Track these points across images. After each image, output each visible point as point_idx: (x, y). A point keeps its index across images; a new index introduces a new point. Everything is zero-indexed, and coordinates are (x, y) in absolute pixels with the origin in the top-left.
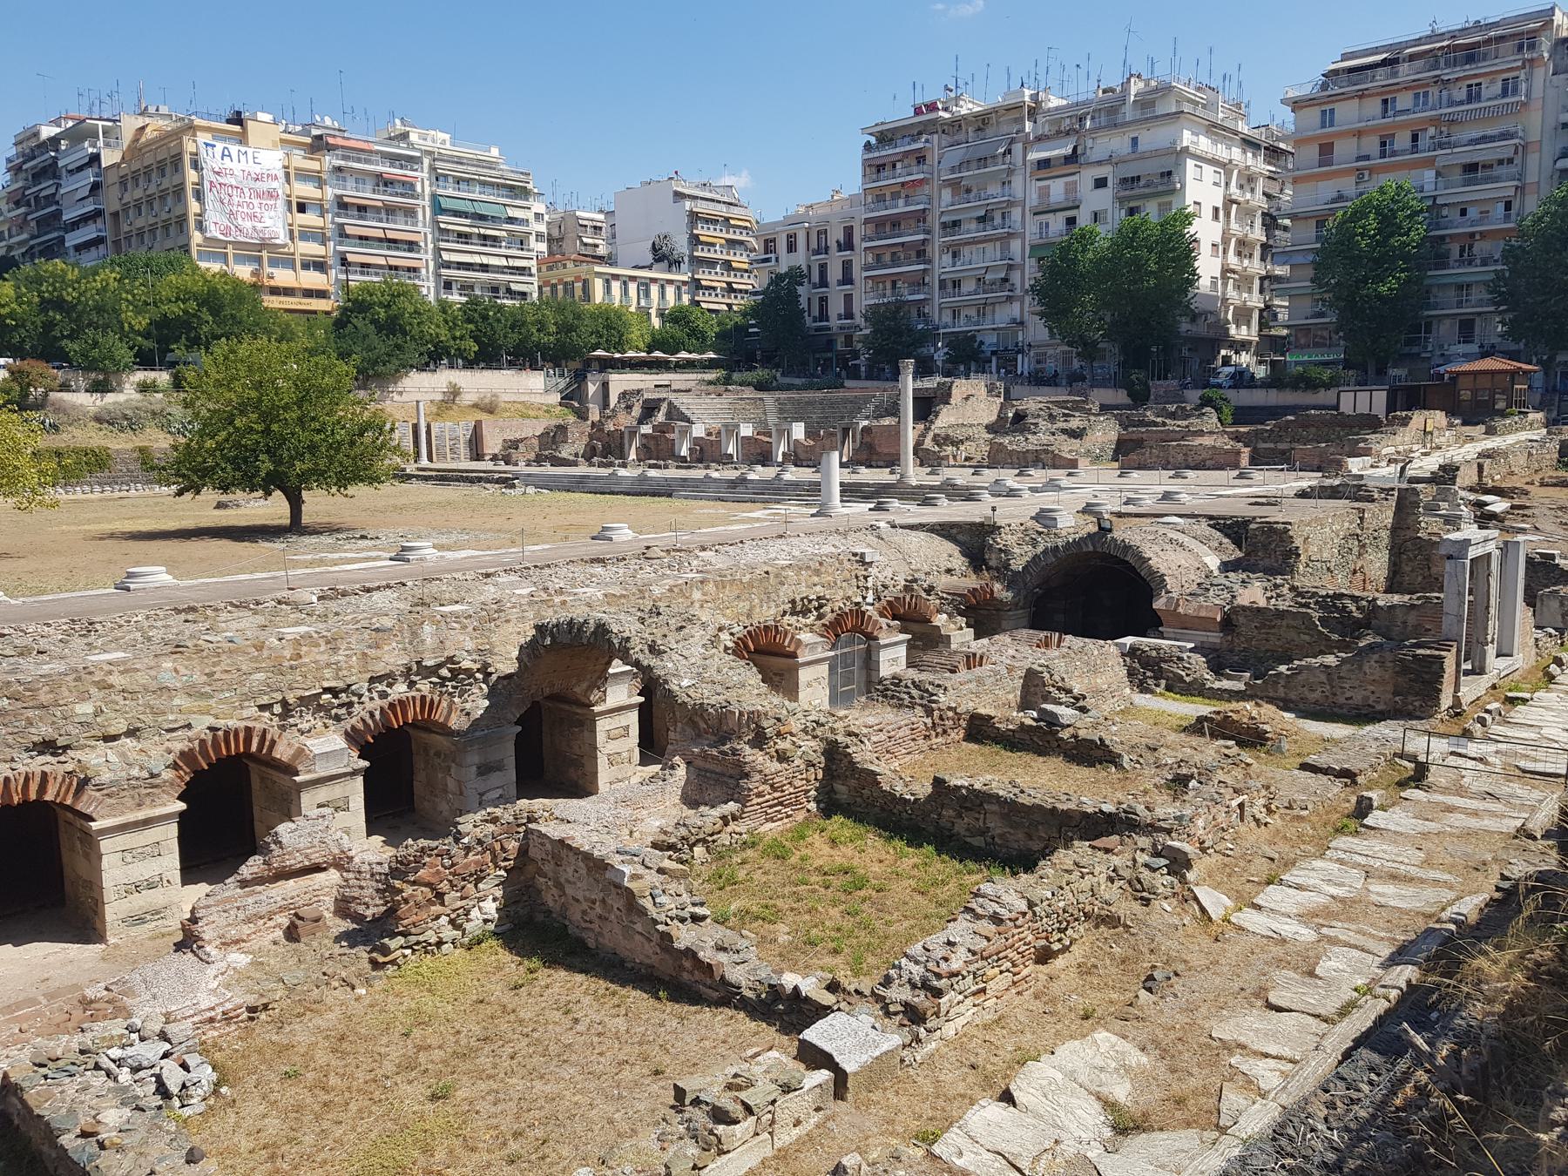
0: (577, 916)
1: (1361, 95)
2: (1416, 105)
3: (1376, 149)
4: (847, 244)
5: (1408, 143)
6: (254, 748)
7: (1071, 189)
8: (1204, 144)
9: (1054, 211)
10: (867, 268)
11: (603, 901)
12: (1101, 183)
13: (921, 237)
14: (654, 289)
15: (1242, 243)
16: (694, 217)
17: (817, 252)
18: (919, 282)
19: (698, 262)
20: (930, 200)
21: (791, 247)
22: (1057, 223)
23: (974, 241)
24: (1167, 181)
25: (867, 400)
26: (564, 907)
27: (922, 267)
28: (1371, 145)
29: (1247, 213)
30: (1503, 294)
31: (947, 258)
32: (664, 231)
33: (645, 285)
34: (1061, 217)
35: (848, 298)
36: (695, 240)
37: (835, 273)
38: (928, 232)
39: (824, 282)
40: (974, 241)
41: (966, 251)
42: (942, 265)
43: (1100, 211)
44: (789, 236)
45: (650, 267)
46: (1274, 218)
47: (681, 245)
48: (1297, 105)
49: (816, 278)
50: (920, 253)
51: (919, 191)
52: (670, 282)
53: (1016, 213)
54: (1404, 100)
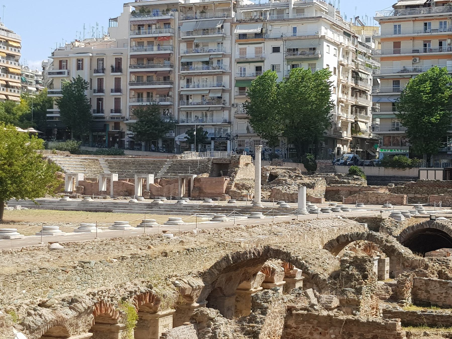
1: (415, 20)
2: (441, 27)
3: (421, 47)
4: (117, 68)
5: (437, 46)
7: (259, 51)
8: (329, 34)
9: (249, 62)
10: (131, 84)
12: (276, 50)
13: (168, 69)
15: (344, 87)
17: (97, 71)
20: (173, 48)
21: (79, 67)
22: (250, 69)
23: (202, 75)
24: (313, 54)
27: (169, 86)
28: (419, 45)
29: (346, 70)
31: (183, 83)
37: (109, 84)
38: (171, 66)
39: (100, 90)
40: (202, 75)
42: (180, 85)
43: (277, 67)
46: (357, 74)
48: (382, 21)
50: (166, 78)
51: (165, 43)
53: (226, 61)
54: (435, 25)
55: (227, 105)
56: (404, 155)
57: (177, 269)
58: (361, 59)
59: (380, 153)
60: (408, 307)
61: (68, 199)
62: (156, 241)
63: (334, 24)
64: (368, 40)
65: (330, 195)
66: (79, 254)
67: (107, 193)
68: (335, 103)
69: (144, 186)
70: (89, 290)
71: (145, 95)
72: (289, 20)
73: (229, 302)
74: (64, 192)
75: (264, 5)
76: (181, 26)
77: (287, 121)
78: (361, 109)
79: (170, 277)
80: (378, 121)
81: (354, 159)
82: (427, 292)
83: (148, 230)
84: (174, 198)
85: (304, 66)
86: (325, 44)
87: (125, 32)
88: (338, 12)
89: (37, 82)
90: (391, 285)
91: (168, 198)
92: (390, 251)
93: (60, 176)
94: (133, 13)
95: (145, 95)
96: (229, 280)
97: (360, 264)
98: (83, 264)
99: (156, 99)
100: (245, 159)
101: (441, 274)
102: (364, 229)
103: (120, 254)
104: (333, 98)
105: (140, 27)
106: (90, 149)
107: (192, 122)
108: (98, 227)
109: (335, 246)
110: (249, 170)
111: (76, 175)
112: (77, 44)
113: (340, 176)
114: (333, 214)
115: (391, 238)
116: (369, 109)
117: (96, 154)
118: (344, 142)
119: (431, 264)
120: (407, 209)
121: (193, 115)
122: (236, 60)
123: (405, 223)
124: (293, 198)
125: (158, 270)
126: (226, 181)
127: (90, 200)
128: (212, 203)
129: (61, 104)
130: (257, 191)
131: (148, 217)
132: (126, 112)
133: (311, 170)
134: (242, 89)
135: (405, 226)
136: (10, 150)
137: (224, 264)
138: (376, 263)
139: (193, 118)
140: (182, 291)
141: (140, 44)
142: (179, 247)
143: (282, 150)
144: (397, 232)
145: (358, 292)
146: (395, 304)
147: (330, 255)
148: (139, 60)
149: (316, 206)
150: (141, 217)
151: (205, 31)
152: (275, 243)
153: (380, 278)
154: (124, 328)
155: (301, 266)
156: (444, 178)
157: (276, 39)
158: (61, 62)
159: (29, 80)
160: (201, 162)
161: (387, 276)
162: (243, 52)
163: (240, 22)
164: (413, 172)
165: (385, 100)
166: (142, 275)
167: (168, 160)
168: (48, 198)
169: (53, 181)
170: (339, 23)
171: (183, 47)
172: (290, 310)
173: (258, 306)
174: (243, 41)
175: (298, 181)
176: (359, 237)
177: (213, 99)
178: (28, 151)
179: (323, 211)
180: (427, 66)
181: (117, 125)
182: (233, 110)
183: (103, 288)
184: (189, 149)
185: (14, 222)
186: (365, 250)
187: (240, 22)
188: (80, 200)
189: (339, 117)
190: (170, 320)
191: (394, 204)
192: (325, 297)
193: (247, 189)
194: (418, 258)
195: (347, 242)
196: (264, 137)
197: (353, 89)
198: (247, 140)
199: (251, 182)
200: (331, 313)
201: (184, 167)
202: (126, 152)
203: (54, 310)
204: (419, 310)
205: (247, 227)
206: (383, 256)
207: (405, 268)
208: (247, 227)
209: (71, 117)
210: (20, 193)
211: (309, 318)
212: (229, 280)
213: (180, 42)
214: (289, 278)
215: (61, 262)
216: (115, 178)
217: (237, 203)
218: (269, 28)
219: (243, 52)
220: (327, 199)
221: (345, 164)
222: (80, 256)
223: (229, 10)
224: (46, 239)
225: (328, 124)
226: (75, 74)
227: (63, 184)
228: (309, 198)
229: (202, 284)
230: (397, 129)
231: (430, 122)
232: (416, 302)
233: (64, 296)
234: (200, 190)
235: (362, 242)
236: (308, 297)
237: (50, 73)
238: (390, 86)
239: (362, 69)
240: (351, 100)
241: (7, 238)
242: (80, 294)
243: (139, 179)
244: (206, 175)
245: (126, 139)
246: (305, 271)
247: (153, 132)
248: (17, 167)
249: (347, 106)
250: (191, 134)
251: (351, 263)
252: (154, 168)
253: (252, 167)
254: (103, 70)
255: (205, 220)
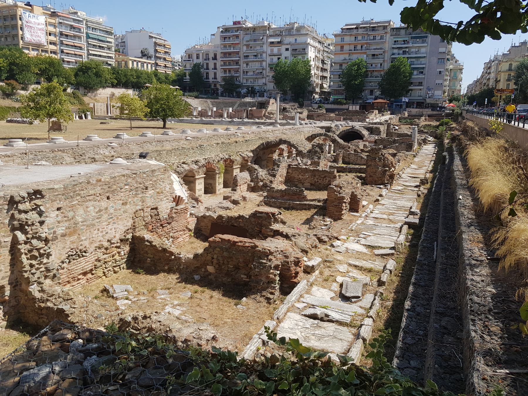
4: (215, 58)
10: (221, 66)
12: (287, 49)
14: (145, 65)
16: (156, 44)
17: (206, 60)
18: (237, 71)
19: (157, 58)
20: (240, 49)
21: (198, 58)
22: (275, 59)
23: (253, 61)
24: (304, 52)
25: (236, 103)
29: (318, 60)
30: (380, 85)
31: (245, 65)
32: (145, 47)
33: (143, 63)
34: (277, 57)
35: (215, 74)
36: (156, 51)
37: (211, 66)
38: (239, 57)
39: (208, 69)
40: (253, 61)
41: (250, 64)
44: (197, 54)
45: (141, 58)
47: (151, 52)
49: (205, 67)
50: (237, 63)
51: (237, 46)
52: (149, 63)
53: (264, 55)
55: (265, 76)
56: (343, 99)
57: (241, 148)
58: (325, 54)
59: (332, 98)
60: (340, 164)
61: (194, 119)
62: (233, 137)
63: (314, 37)
64: (329, 45)
65: (309, 117)
66: (199, 142)
67: (211, 116)
68: (313, 74)
69: (228, 113)
70: (204, 157)
71: (228, 71)
72: (293, 35)
73: (264, 163)
74: (192, 115)
75: (282, 28)
76: (244, 38)
77: (291, 83)
78: (324, 78)
79: (238, 152)
80: (332, 83)
81: (320, 101)
82: (349, 158)
83: (229, 132)
84: (241, 119)
85: (300, 57)
86: (310, 47)
87: (218, 41)
88: (316, 31)
89: (179, 65)
90: (333, 155)
91: (238, 119)
92: (334, 141)
93: (190, 108)
94: (222, 32)
95: (228, 71)
96: (264, 153)
97: (320, 146)
98: (201, 146)
99: (233, 74)
100: (272, 101)
101: (355, 151)
102: (323, 131)
103: (217, 142)
104: (312, 72)
105: (225, 38)
106: (204, 96)
107: (249, 84)
108: (207, 130)
109: (310, 139)
110: (274, 106)
111: (197, 108)
112: (196, 47)
113: (314, 109)
114: (310, 125)
115: (334, 135)
116: (328, 78)
117: (206, 98)
118: (316, 93)
119: (351, 147)
120: (343, 123)
121: (249, 80)
122: (269, 54)
123: (341, 129)
124: (293, 118)
125: (234, 148)
126: (264, 110)
127: (204, 119)
128: (257, 120)
129: (190, 75)
130: (277, 115)
131: (229, 127)
132: (219, 79)
133: (301, 106)
134: (271, 68)
135: (341, 131)
136: (168, 97)
137: (262, 147)
138: (328, 147)
139: (249, 82)
140: (244, 158)
141: (225, 46)
142: (242, 139)
143: (289, 97)
144: (338, 133)
145: (319, 158)
146: (335, 164)
147: (308, 142)
148: (225, 54)
149: (303, 122)
150: (225, 127)
151: (255, 40)
152: (284, 137)
153: (329, 153)
154: (219, 173)
155: (295, 147)
156: (360, 109)
157: (287, 44)
158: (189, 55)
159: (175, 64)
160: (253, 102)
161: (332, 152)
162: (272, 50)
163: (271, 36)
164: (346, 107)
165: (335, 73)
166: (226, 151)
167: (238, 101)
168: (186, 118)
169: (188, 111)
170: (316, 37)
171: (245, 48)
172: (289, 165)
173: (276, 164)
174: (272, 45)
175: (296, 111)
176: (321, 135)
177: (258, 73)
178: (175, 97)
179: (306, 124)
180: (355, 58)
181: (215, 85)
182: (267, 78)
183: (210, 156)
184: (248, 96)
185: (171, 128)
186: (323, 141)
187: (271, 36)
188: (199, 119)
189: (315, 82)
190: (238, 170)
191: (337, 121)
192: (305, 160)
193: (273, 114)
194: (346, 144)
195: (316, 137)
196: (281, 91)
197: (321, 68)
198: (273, 92)
199: (275, 111)
200: (307, 167)
201: (246, 104)
202: (219, 98)
203: (189, 165)
204: (344, 166)
205: (272, 131)
206: (331, 143)
207: (340, 148)
208: (272, 131)
209: (195, 80)
210: (173, 116)
211: (297, 169)
212: (264, 153)
213: (243, 46)
214: (290, 152)
215: (191, 145)
216: (215, 109)
217: (268, 121)
218: (284, 39)
219: (272, 50)
220: (308, 119)
221: (316, 103)
222: (199, 142)
223: (266, 30)
224: (184, 135)
225: (310, 85)
226: (196, 61)
227: (192, 112)
228: (300, 118)
229: (252, 155)
230: (340, 87)
231: (355, 84)
232: (343, 163)
233: (193, 159)
234: (252, 115)
235: (322, 137)
236: (298, 161)
237: (184, 61)
238: (338, 67)
239: (326, 59)
240: (321, 74)
241: (168, 134)
242: (200, 159)
243: (225, 110)
244: (255, 108)
245: (219, 92)
246: (297, 150)
247: (231, 89)
248: (171, 103)
249: (318, 76)
250: (248, 89)
251: (317, 146)
252: (232, 105)
253: (275, 105)
254: (209, 59)
255: (254, 128)
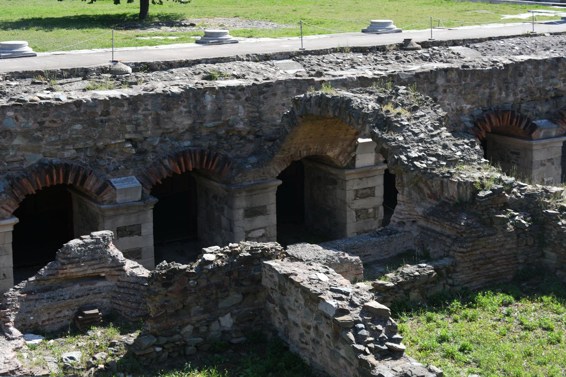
0: (296, 338)
6: (70, 182)
11: (316, 328)
26: (287, 331)
